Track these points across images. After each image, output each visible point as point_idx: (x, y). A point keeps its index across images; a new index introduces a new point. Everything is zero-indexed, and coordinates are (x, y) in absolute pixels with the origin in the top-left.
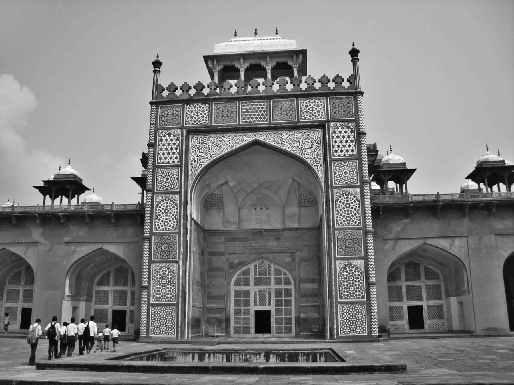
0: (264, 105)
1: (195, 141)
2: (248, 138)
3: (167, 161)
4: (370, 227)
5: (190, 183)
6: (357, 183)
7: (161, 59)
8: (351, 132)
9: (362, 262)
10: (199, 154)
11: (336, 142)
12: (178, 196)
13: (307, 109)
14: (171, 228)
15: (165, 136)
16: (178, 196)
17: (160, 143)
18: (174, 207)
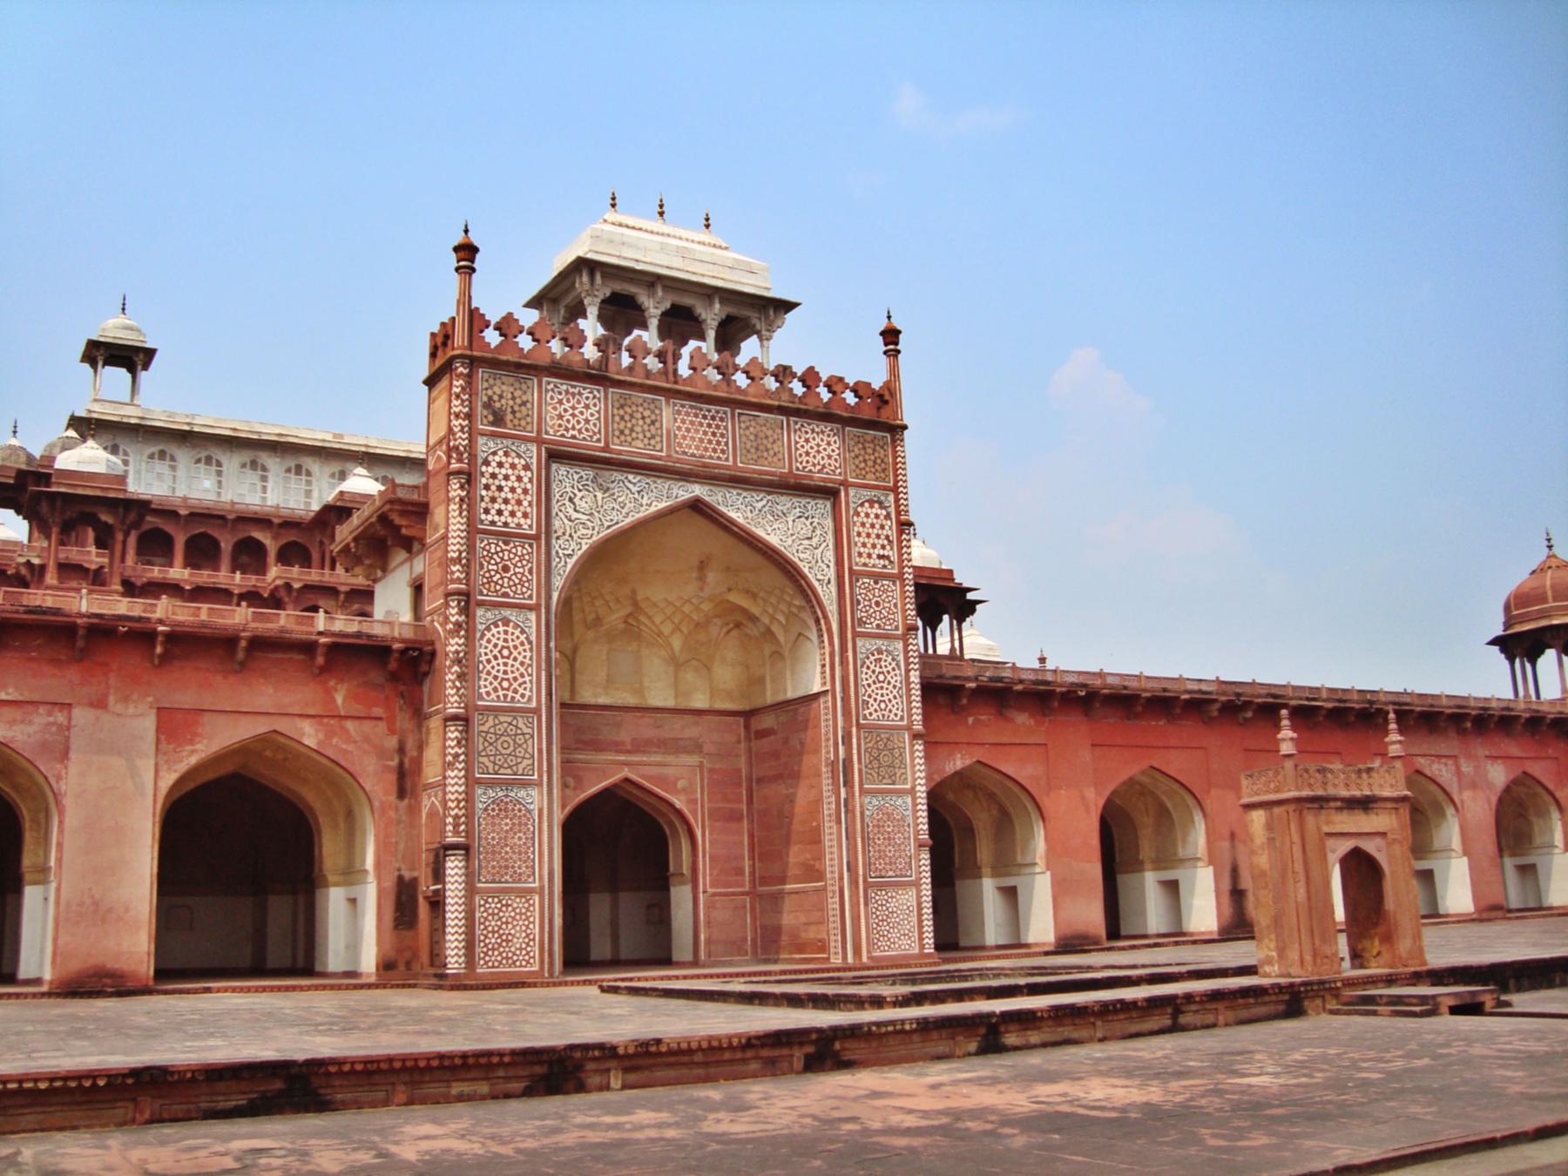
0: (722, 419)
1: (565, 478)
2: (685, 492)
3: (503, 519)
4: (918, 727)
5: (558, 582)
6: (897, 628)
7: (475, 239)
8: (888, 517)
9: (909, 800)
10: (575, 515)
11: (859, 534)
12: (533, 616)
13: (807, 447)
14: (518, 697)
15: (494, 453)
16: (533, 616)
17: (484, 469)
18: (522, 644)
